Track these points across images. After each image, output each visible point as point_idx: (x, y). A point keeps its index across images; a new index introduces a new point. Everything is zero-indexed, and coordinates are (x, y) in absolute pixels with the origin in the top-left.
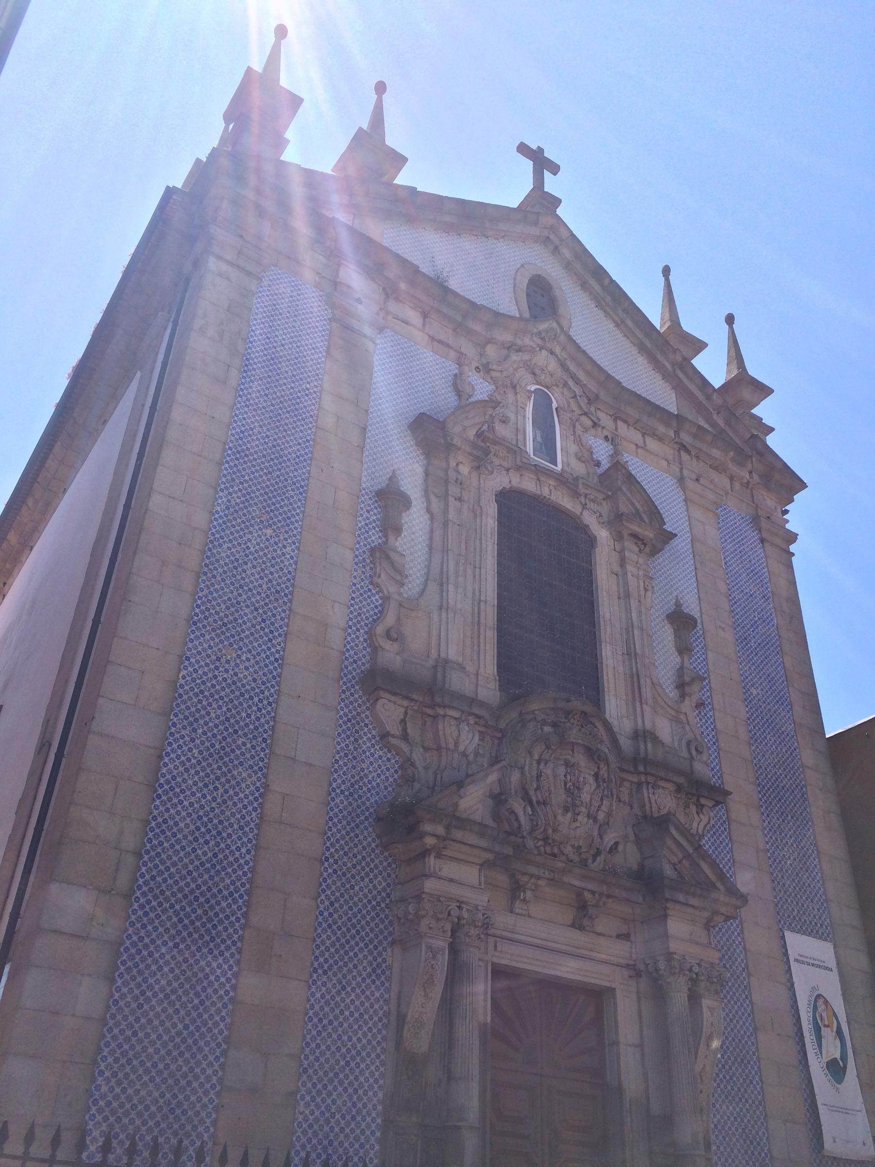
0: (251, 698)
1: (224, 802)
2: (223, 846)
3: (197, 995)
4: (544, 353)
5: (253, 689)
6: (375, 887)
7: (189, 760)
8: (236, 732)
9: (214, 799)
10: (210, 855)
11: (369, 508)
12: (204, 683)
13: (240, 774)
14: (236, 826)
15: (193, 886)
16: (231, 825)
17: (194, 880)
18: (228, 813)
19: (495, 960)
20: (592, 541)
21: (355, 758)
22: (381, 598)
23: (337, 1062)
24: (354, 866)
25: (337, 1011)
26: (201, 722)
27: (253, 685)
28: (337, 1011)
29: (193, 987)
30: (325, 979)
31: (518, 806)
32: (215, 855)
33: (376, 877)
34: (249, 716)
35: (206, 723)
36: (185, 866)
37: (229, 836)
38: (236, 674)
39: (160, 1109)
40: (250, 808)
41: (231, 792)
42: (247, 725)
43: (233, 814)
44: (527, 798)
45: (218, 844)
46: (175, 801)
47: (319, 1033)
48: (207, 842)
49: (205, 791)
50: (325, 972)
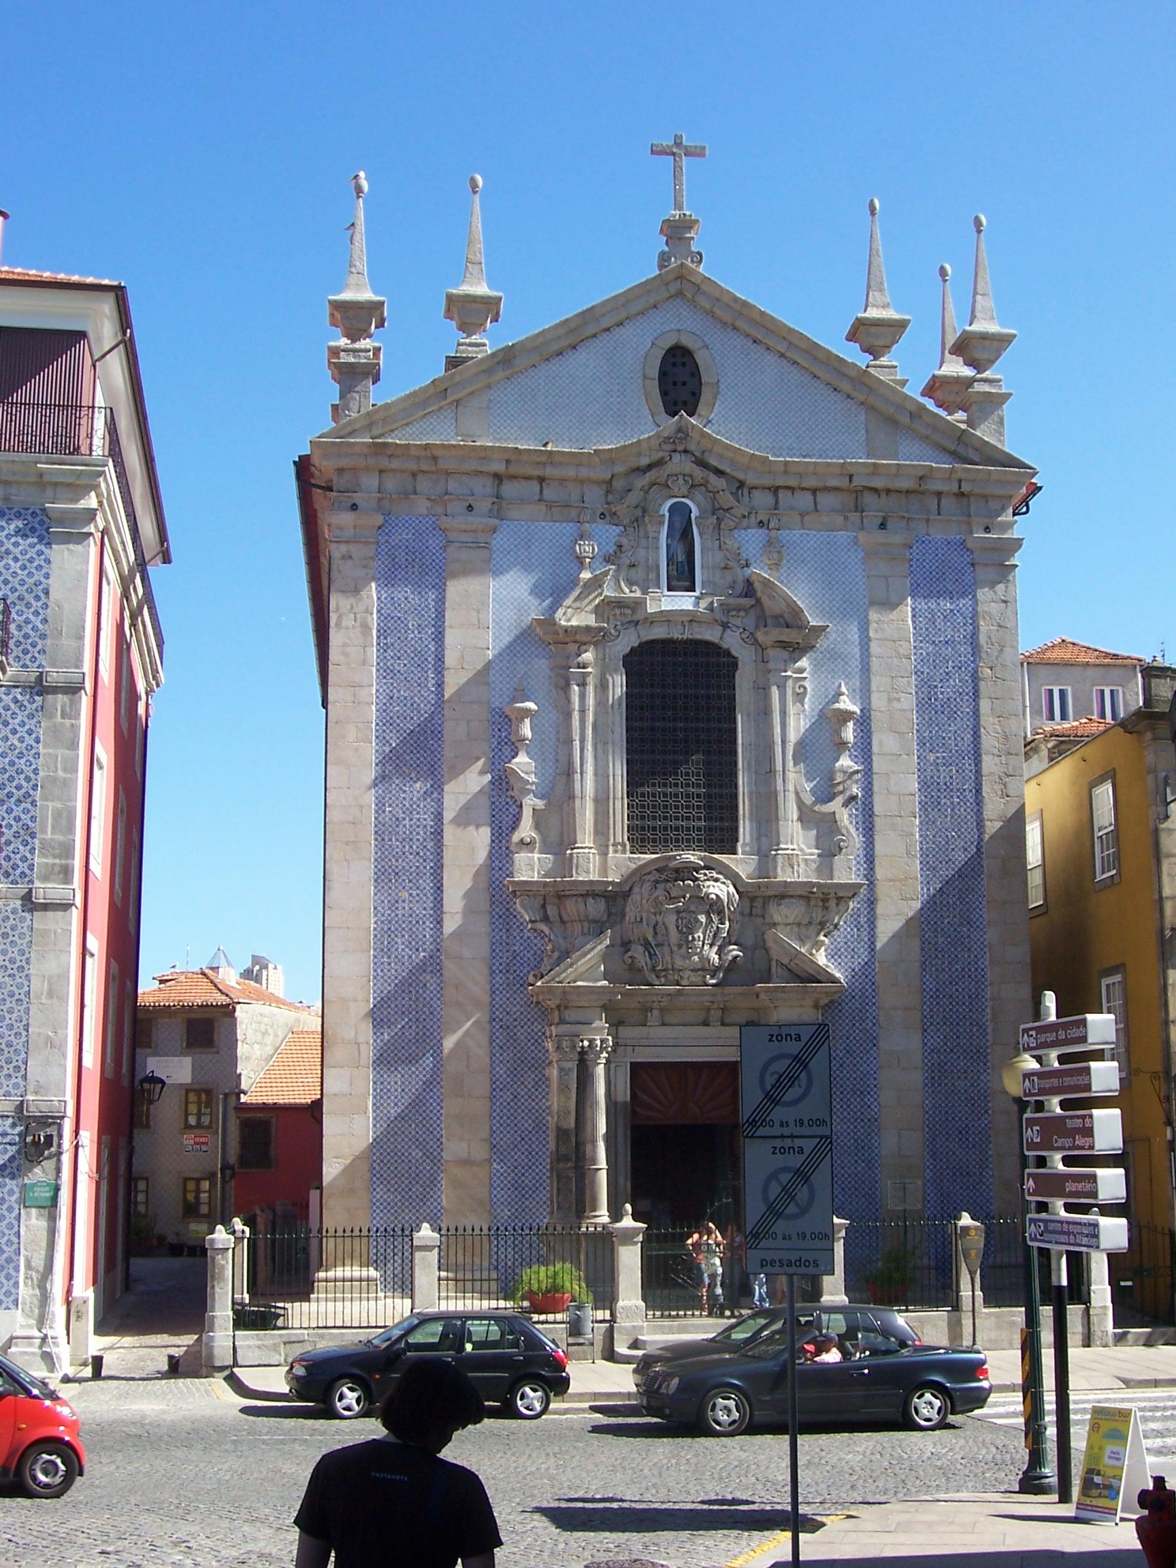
0: (424, 923)
1: (417, 999)
2: (421, 1027)
3: (421, 1115)
4: (677, 457)
5: (425, 915)
6: (533, 1030)
7: (389, 978)
8: (417, 950)
9: (410, 999)
10: (414, 1034)
11: (500, 727)
12: (390, 922)
13: (425, 978)
14: (428, 1013)
15: (407, 1055)
16: (424, 1013)
17: (406, 1051)
18: (421, 1006)
19: (634, 1060)
20: (733, 664)
21: (508, 944)
22: (517, 806)
23: (516, 1139)
24: (515, 1020)
25: (512, 1111)
26: (393, 950)
27: (424, 912)
28: (512, 1111)
29: (417, 1111)
30: (501, 1093)
31: (638, 952)
32: (417, 1034)
33: (533, 1024)
34: (425, 936)
35: (397, 950)
36: (400, 1044)
37: (425, 1020)
38: (411, 909)
39: (410, 1175)
40: (435, 999)
41: (421, 991)
42: (424, 943)
43: (424, 1006)
44: (647, 945)
45: (418, 1027)
46: (386, 1006)
47: (501, 1125)
48: (411, 1027)
49: (403, 995)
50: (501, 1090)
